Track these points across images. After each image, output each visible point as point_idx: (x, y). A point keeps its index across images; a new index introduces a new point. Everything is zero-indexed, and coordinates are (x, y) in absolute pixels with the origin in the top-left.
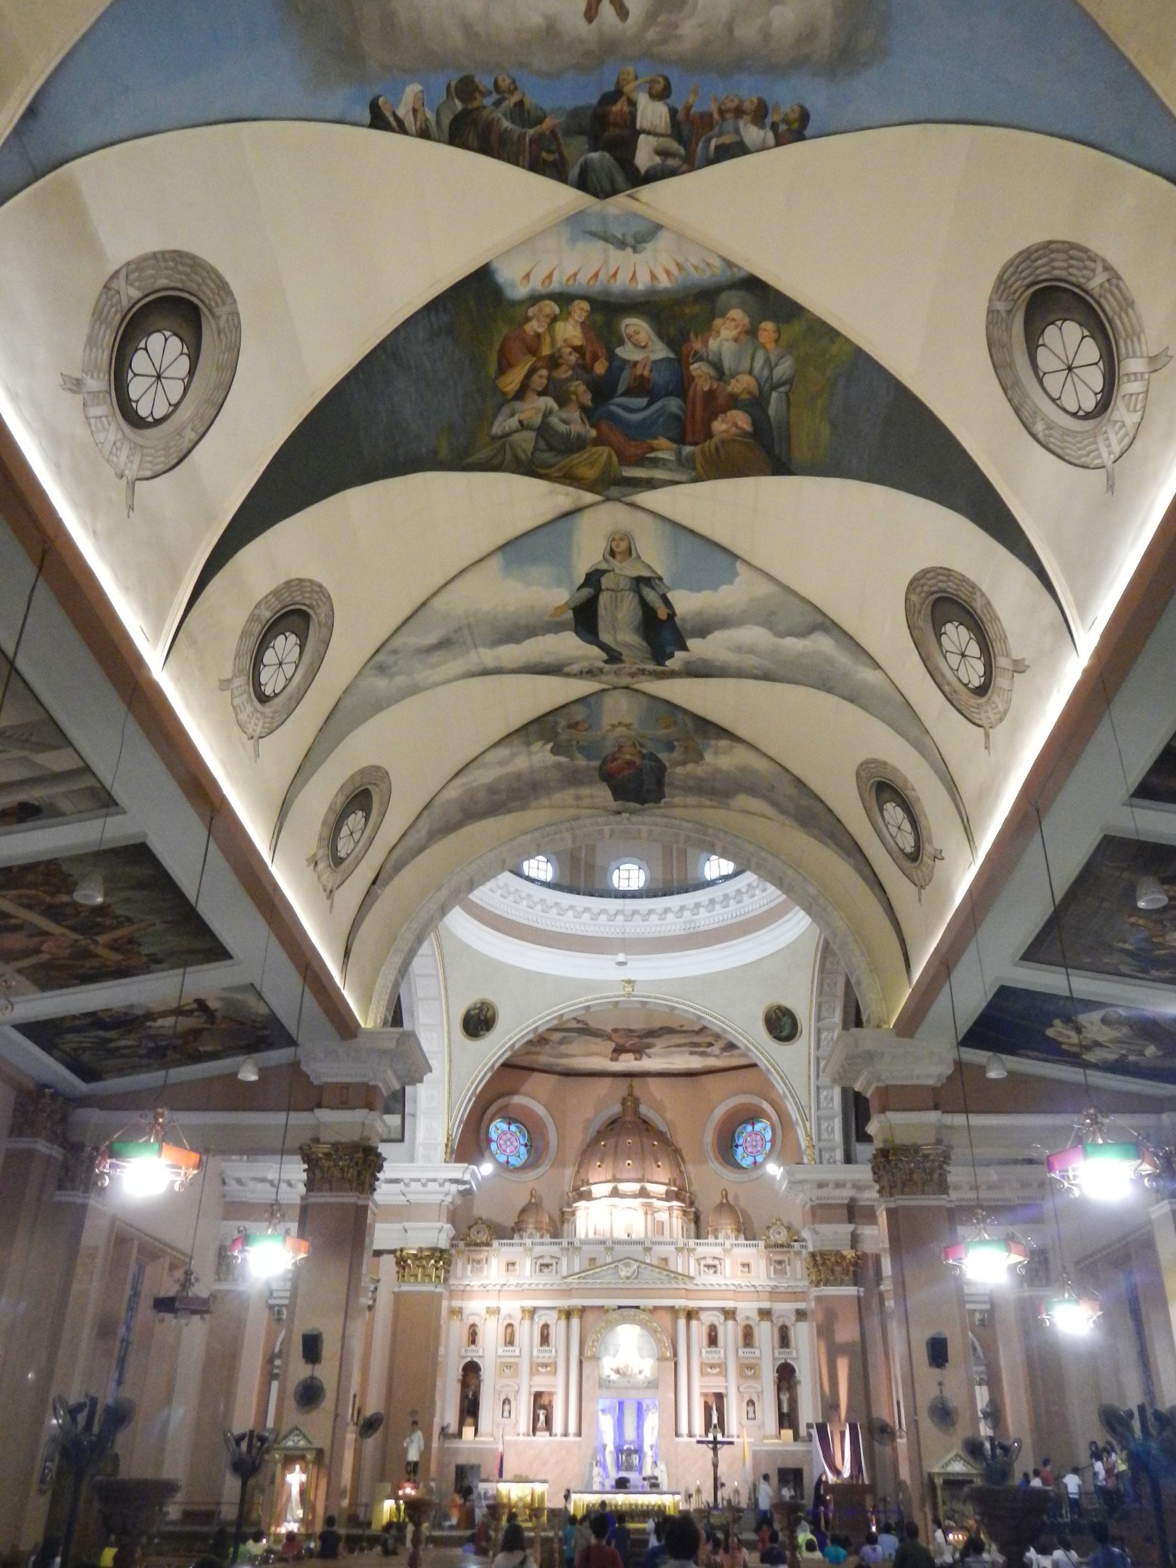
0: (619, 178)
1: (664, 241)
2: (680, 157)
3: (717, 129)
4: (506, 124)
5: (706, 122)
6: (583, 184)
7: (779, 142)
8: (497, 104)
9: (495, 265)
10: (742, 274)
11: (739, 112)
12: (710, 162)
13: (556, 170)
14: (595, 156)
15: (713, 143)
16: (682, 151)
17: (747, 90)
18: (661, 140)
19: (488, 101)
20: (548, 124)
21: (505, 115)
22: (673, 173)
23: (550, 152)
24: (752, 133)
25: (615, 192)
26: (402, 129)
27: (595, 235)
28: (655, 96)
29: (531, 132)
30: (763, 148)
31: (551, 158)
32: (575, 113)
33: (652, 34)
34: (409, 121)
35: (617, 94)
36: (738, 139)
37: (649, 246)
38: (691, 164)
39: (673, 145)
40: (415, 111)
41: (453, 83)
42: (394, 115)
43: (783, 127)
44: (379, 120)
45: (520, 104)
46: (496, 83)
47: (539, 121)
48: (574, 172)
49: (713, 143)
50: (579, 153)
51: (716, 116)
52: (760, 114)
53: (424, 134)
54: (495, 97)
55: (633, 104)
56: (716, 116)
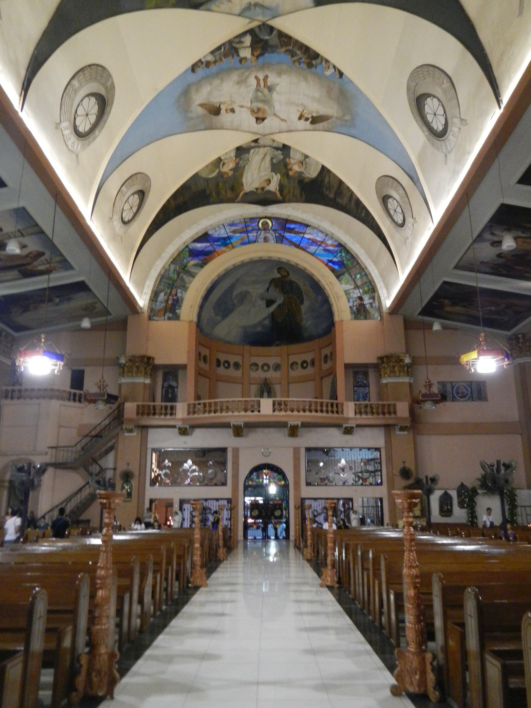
0: (257, 31)
1: (237, 9)
2: (234, 43)
3: (222, 54)
4: (299, 52)
5: (226, 55)
6: (272, 29)
7: (200, 61)
8: (301, 58)
9: (312, 4)
10: (202, 8)
11: (215, 62)
12: (224, 44)
13: (281, 35)
14: (267, 37)
15: (223, 50)
16: (234, 45)
17: (214, 69)
18: (242, 46)
19: (303, 60)
20: (283, 50)
21: (298, 55)
22: (237, 37)
23: (284, 41)
24: (210, 58)
25: (259, 27)
26: (334, 67)
27: (268, 8)
28: (245, 58)
29: (290, 48)
30: (205, 57)
31: (284, 39)
32: (273, 52)
33: (247, 73)
34: (331, 67)
35: (258, 57)
36: (214, 54)
37: (244, 6)
38: (230, 42)
39: (237, 46)
40: (329, 67)
41: (314, 68)
42: (335, 71)
43: (200, 64)
44: (341, 74)
45: (292, 56)
46: (300, 64)
47: (286, 51)
48: (275, 33)
49: (223, 50)
50: (273, 39)
51: (223, 58)
52: (208, 64)
53: (327, 61)
54: (301, 61)
55: (252, 54)
56: (223, 58)
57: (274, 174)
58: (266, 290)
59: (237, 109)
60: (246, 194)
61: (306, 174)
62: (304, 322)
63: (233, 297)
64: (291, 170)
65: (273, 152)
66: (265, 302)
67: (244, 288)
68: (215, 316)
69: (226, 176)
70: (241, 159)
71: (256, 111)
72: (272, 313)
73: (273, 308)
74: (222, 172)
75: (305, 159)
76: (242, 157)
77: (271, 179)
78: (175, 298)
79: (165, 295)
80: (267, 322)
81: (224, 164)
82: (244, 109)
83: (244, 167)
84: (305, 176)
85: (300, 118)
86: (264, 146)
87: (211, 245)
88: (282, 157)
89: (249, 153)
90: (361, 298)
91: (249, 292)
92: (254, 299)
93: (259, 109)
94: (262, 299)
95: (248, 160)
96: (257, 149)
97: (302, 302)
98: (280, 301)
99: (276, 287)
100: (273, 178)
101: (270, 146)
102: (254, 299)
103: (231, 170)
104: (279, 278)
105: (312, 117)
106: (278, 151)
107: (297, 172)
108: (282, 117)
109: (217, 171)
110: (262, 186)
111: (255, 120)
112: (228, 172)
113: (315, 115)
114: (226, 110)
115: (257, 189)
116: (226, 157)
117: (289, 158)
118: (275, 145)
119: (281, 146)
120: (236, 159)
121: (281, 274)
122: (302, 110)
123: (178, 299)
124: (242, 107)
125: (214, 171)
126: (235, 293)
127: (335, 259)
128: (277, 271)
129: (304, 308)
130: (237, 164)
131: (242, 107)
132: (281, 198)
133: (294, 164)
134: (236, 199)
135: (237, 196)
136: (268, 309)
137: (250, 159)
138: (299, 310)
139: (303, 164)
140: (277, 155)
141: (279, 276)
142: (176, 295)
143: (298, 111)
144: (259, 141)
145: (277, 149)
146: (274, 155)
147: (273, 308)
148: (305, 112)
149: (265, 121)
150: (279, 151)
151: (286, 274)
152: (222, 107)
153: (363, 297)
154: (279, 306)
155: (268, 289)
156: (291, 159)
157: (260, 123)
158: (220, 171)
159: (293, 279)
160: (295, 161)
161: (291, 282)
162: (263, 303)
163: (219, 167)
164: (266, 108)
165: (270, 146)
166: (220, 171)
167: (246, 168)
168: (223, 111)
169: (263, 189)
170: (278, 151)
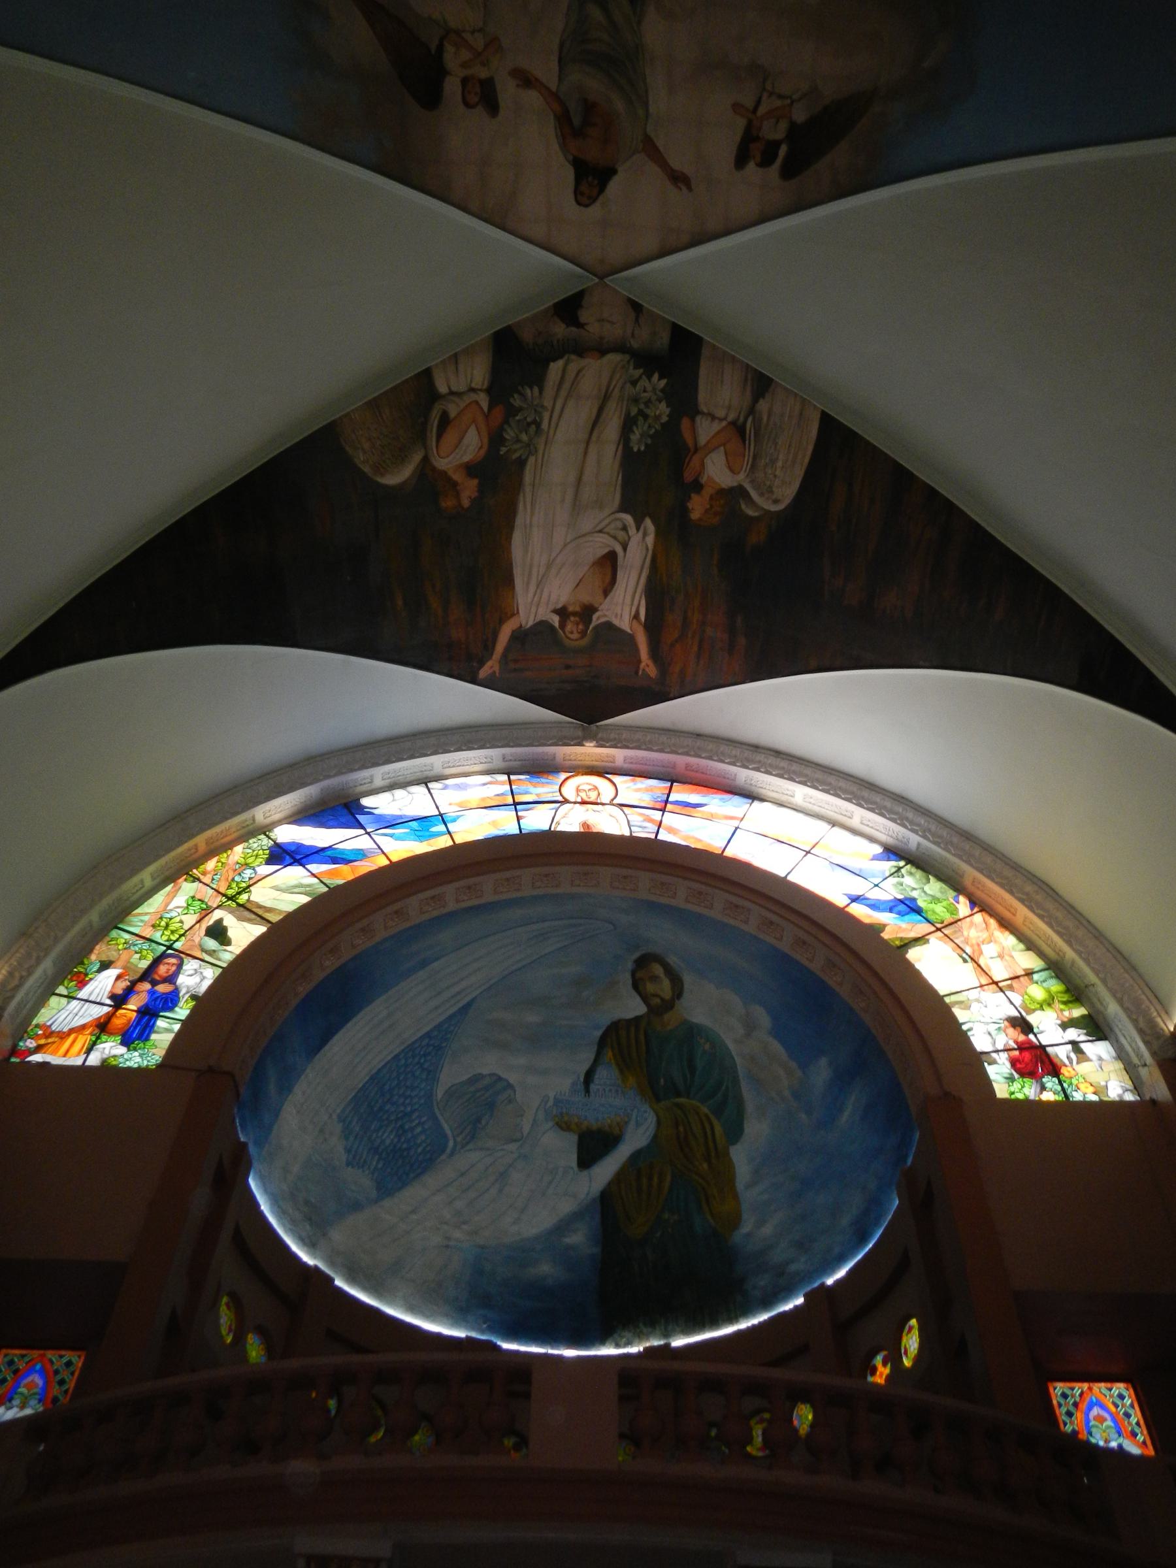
57: (628, 519)
58: (581, 1087)
59: (507, 90)
60: (520, 637)
61: (753, 494)
62: (746, 1227)
63: (440, 1093)
64: (697, 486)
65: (634, 383)
66: (574, 1138)
67: (489, 1063)
68: (348, 1164)
69: (447, 503)
70: (512, 411)
71: (577, 121)
72: (606, 1198)
73: (606, 1170)
74: (434, 469)
75: (752, 411)
76: (517, 401)
77: (619, 549)
78: (162, 988)
79: (119, 977)
80: (579, 1238)
81: (445, 422)
82: (532, 98)
83: (522, 463)
84: (751, 512)
85: (741, 161)
86: (602, 350)
87: (368, 833)
88: (663, 410)
89: (538, 381)
90: (1021, 1024)
91: (510, 1086)
92: (526, 1128)
93: (589, 107)
94: (564, 1126)
95: (538, 425)
96: (575, 364)
97: (735, 1133)
98: (636, 1139)
99: (625, 1064)
100: (625, 549)
101: (621, 348)
102: (526, 1128)
103: (470, 469)
104: (637, 1019)
105: (793, 128)
106: (649, 378)
107: (722, 493)
108: (676, 163)
109: (417, 458)
110: (586, 598)
111: (569, 174)
112: (457, 477)
113: (800, 115)
114: (465, 81)
115: (562, 612)
116: (454, 389)
117: (692, 410)
118: (641, 338)
119: (664, 339)
120: (490, 408)
121: (645, 999)
122: (749, 103)
123: (176, 991)
124: (526, 80)
125: (401, 457)
126: (451, 1075)
127: (875, 895)
128: (630, 965)
129: (741, 1157)
130: (496, 439)
131: (526, 80)
132: (652, 671)
133: (710, 448)
134: (482, 663)
135: (488, 646)
136: (585, 1173)
137: (545, 425)
138: (724, 1175)
139: (744, 441)
140: (648, 403)
141: (634, 1007)
142: (171, 979)
143: (737, 107)
144: (584, 316)
145: (646, 361)
146: (636, 400)
147: (606, 1170)
148: (761, 111)
149: (614, 186)
150: (656, 376)
151: (665, 988)
152: (453, 58)
153: (1032, 1019)
154: (636, 1156)
155: (589, 1077)
156: (698, 419)
157: (593, 200)
158: (426, 459)
159: (699, 1017)
160: (716, 426)
161: (692, 1032)
162: (564, 1148)
163: (421, 436)
164: (619, 105)
165: (621, 348)
166: (426, 459)
167: (528, 477)
168: (452, 87)
169: (588, 611)
170: (649, 378)
